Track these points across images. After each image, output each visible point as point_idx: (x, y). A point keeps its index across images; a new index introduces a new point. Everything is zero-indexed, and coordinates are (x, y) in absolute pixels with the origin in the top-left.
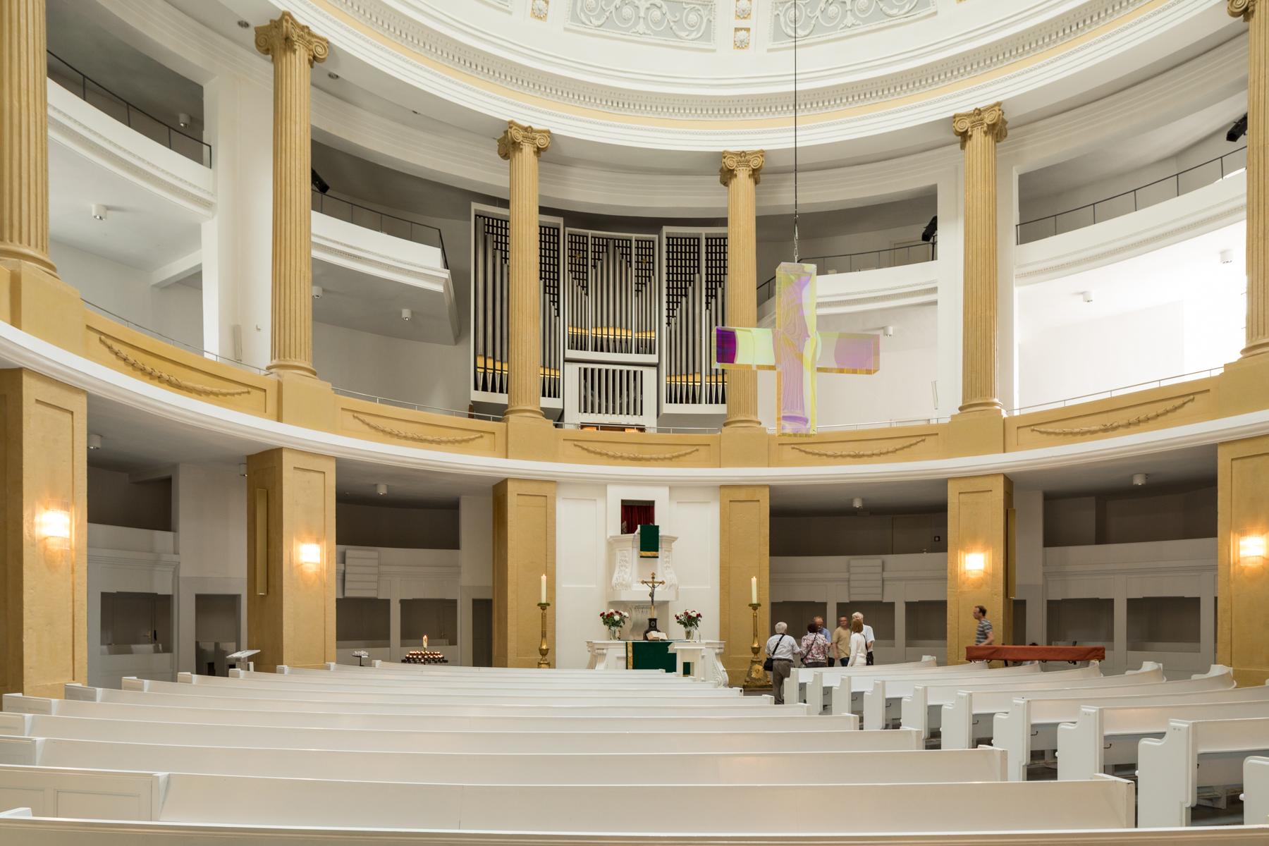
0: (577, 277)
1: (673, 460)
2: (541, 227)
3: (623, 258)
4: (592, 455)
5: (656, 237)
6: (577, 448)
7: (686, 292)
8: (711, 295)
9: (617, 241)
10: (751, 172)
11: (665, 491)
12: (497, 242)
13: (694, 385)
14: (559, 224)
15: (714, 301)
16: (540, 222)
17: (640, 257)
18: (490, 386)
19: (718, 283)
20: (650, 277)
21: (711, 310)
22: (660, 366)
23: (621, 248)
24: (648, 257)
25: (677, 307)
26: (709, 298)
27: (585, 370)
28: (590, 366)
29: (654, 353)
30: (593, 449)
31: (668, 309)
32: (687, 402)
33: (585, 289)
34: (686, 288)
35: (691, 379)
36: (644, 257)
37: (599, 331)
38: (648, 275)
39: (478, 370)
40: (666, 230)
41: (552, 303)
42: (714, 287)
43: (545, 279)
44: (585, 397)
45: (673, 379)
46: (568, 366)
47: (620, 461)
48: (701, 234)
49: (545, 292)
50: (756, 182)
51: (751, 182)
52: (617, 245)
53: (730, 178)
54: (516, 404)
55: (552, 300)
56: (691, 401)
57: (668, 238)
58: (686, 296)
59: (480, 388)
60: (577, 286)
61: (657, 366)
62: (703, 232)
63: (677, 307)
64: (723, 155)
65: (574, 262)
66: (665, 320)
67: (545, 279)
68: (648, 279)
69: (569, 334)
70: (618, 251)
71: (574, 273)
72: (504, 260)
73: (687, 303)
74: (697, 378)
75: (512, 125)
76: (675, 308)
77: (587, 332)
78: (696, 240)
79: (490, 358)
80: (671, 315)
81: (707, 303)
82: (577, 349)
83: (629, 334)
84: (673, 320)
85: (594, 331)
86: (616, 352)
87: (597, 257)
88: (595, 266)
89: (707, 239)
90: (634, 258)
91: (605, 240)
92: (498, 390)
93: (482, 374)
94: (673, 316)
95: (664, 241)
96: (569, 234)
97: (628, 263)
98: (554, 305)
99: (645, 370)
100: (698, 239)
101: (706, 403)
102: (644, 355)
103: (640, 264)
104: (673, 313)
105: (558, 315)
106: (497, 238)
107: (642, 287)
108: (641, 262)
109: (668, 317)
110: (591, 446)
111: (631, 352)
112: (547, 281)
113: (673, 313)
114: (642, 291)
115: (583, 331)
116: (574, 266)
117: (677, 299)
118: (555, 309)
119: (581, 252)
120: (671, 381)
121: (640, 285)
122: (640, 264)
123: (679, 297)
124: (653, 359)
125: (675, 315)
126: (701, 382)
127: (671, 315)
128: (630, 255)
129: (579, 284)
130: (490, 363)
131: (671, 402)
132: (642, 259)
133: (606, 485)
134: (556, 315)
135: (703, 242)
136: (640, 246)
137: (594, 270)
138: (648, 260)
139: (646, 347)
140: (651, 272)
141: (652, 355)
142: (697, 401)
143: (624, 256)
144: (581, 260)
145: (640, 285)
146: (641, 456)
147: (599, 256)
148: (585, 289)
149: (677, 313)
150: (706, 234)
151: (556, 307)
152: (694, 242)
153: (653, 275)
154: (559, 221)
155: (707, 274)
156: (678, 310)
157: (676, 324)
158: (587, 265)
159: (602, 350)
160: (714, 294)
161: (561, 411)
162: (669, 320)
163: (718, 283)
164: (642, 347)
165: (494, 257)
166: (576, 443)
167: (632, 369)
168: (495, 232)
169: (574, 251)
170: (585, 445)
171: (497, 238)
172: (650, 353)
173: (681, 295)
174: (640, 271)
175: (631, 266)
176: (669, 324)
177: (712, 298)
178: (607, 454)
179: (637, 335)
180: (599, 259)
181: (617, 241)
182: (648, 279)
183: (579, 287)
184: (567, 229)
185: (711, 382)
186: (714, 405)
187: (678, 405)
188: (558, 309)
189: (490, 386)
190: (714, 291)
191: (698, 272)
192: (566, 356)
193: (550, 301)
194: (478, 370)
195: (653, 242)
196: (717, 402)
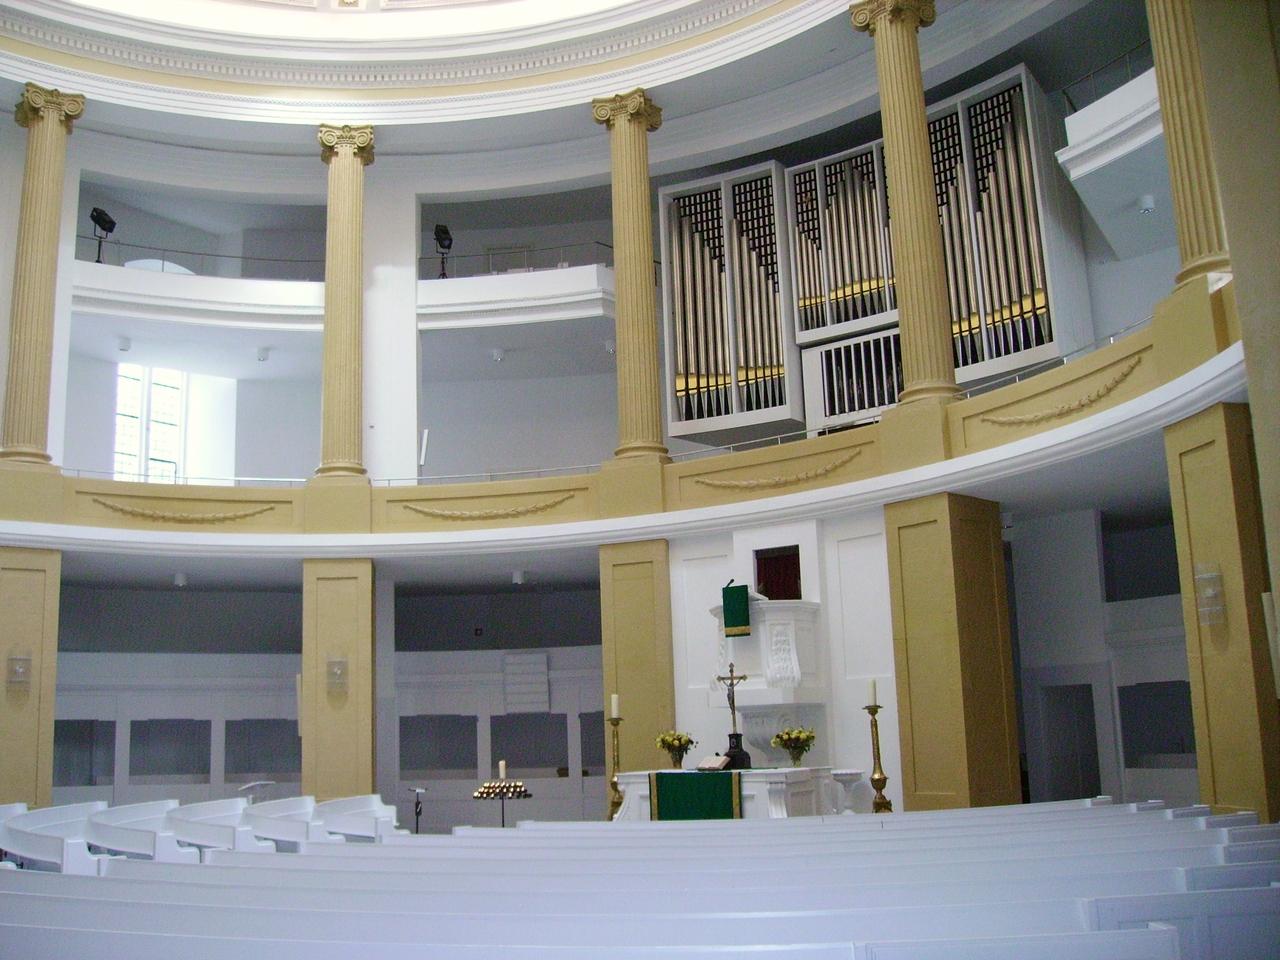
1: (829, 475)
14: (770, 170)
28: (832, 347)
88: (828, 205)
146: (783, 479)
154: (771, 166)
175: (875, 187)
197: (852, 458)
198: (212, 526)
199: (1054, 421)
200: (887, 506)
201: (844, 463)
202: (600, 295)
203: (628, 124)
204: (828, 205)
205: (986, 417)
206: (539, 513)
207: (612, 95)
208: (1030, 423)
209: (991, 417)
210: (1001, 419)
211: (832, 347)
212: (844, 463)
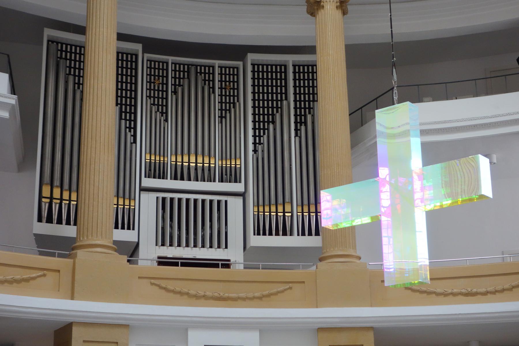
0: (156, 103)
1: (263, 299)
2: (118, 53)
3: (205, 84)
4: (171, 294)
5: (240, 64)
6: (154, 286)
7: (273, 118)
8: (300, 122)
9: (199, 67)
10: (339, 4)
11: (256, 335)
12: (70, 67)
13: (284, 216)
14: (138, 50)
15: (303, 128)
16: (118, 48)
17: (223, 83)
18: (55, 217)
19: (307, 110)
20: (234, 103)
21: (300, 137)
22: (247, 195)
23: (203, 75)
24: (232, 84)
25: (264, 134)
26: (299, 124)
27: (164, 199)
28: (169, 195)
29: (240, 182)
31: (254, 136)
32: (277, 234)
33: (164, 115)
34: (273, 115)
35: (280, 209)
36: (228, 83)
37: (179, 159)
38: (232, 101)
39: (43, 200)
40: (251, 57)
41: (128, 130)
42: (303, 113)
43: (121, 104)
44: (163, 229)
45: (261, 209)
46: (144, 195)
47: (202, 301)
48: (289, 61)
49: (121, 118)
50: (344, 13)
51: (338, 14)
52: (199, 71)
53: (317, 9)
54: (86, 238)
55: (128, 126)
56: (281, 233)
57: (253, 65)
58: (273, 122)
59: (44, 220)
60: (156, 112)
61: (243, 195)
62: (290, 59)
63: (264, 134)
65: (152, 88)
66: (251, 147)
67: (121, 104)
68: (232, 105)
69: (145, 162)
70: (200, 78)
71: (152, 99)
72: (76, 85)
73: (275, 129)
74: (288, 208)
76: (262, 134)
77: (166, 159)
78: (283, 67)
79: (57, 186)
80: (257, 141)
81: (296, 130)
82: (154, 177)
83: (212, 161)
84: (260, 147)
85: (174, 159)
86: (197, 180)
87: (177, 83)
88: (175, 92)
89: (294, 66)
90: (217, 85)
91: (186, 66)
92: (64, 222)
93: (47, 205)
94: (260, 143)
95: (249, 68)
96: (147, 60)
97: (211, 90)
98: (130, 131)
99: (230, 199)
100: (285, 66)
101: (298, 235)
102: (229, 184)
103: (224, 90)
104: (260, 140)
105: (135, 142)
106: (70, 64)
107: (226, 113)
108: (225, 89)
109: (255, 143)
110: (170, 285)
111: (214, 181)
112: (124, 107)
113: (260, 140)
114: (225, 117)
115: (162, 159)
116: (152, 92)
117: (264, 125)
118: (132, 136)
119: (161, 78)
120: (258, 212)
121: (224, 112)
122: (224, 90)
123: (266, 124)
124: (239, 187)
125: (262, 142)
126: (292, 212)
127: (257, 141)
128: (213, 81)
129: (158, 110)
130: (57, 193)
131: (259, 234)
132: (226, 85)
133: (186, 330)
134: (132, 141)
135: (291, 69)
136: (223, 72)
137: (174, 96)
138: (232, 87)
139: (231, 175)
140: (236, 98)
142: (288, 233)
143: (207, 82)
144: (161, 85)
145: (224, 112)
146: (227, 295)
147: (179, 82)
148: (164, 115)
149: (264, 139)
150: (293, 61)
151: (132, 134)
152: (281, 69)
153: (238, 101)
154: (138, 47)
155: (295, 101)
156: (265, 137)
157: (263, 151)
158: (167, 91)
159: (182, 179)
160: (303, 121)
161: (135, 244)
162: (255, 147)
163: (307, 110)
164: (226, 175)
165: (66, 82)
166: (153, 281)
167: (216, 198)
168: (68, 57)
169: (152, 77)
170: (163, 283)
171: (70, 64)
172: (236, 181)
173: (268, 122)
174: (224, 97)
175: (214, 92)
176: (255, 151)
177: (301, 125)
178: (187, 294)
179: (220, 163)
180: (179, 85)
181: (199, 67)
182: (232, 105)
183: (158, 113)
184: (147, 56)
185: (303, 212)
186: (307, 237)
187: (267, 237)
188: (135, 136)
189: (55, 217)
190: (303, 117)
191: (286, 99)
192: (143, 185)
193: (126, 128)
194: (43, 200)
195: (237, 68)
196: (310, 234)
198: (494, 296)
199: (460, 297)
200: (321, 330)
204: (175, 92)
206: (15, 284)
208: (438, 294)
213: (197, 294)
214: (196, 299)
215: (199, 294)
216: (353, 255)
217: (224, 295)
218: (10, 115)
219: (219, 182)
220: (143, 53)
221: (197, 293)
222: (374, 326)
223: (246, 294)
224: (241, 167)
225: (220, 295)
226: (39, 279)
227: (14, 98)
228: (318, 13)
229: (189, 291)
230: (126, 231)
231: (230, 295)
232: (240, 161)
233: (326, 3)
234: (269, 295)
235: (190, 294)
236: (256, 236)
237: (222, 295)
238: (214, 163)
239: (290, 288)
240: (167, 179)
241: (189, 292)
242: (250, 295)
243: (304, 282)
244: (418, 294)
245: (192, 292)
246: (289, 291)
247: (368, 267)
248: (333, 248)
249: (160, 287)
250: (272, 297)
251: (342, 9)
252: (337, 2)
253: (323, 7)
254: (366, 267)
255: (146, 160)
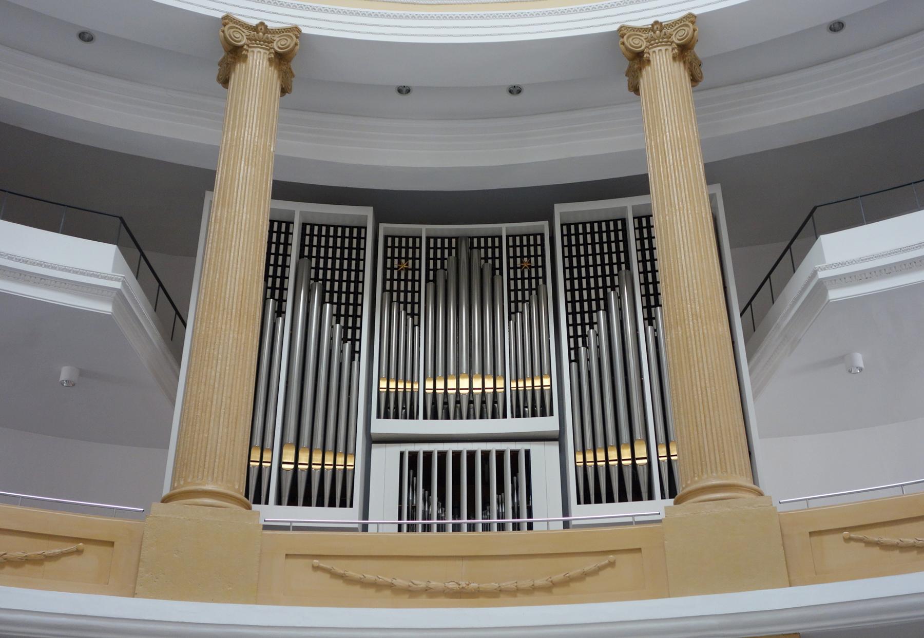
1: (555, 590)
4: (357, 589)
5: (545, 224)
6: (319, 574)
10: (676, 51)
24: (533, 259)
28: (421, 448)
30: (358, 576)
40: (561, 210)
46: (377, 450)
47: (423, 599)
56: (630, 495)
61: (558, 438)
64: (622, 32)
69: (379, 393)
75: (227, 21)
77: (416, 386)
78: (619, 223)
85: (429, 385)
99: (534, 447)
110: (353, 569)
111: (505, 416)
124: (549, 424)
126: (649, 457)
131: (587, 501)
141: (548, 418)
146: (474, 585)
154: (367, 212)
166: (316, 562)
170: (338, 566)
172: (543, 414)
178: (391, 586)
184: (382, 226)
197: (601, 569)
201: (585, 575)
202: (118, 285)
203: (266, 63)
205: (853, 535)
207: (254, 22)
209: (872, 535)
210: (886, 539)
211: (421, 448)
212: (585, 575)
213: (409, 586)
214: (410, 597)
215: (415, 586)
216: (741, 486)
217: (468, 585)
218: (113, 308)
219: (512, 417)
220: (378, 220)
221: (410, 584)
222: (800, 632)
223: (515, 581)
224: (551, 389)
225: (461, 586)
226: (64, 559)
227: (120, 279)
228: (641, 76)
229: (394, 580)
230: (337, 510)
231: (481, 586)
232: (549, 379)
233: (654, 55)
234: (567, 582)
235: (395, 586)
236: (583, 507)
237: (464, 586)
238: (503, 386)
239: (612, 564)
240: (417, 418)
241: (394, 581)
242: (525, 584)
243: (639, 550)
244: (897, 553)
245: (400, 582)
246: (609, 569)
247: (775, 504)
248: (698, 476)
249: (334, 575)
250: (574, 585)
251: (684, 63)
252: (673, 49)
253: (649, 61)
254: (772, 505)
255: (381, 390)
